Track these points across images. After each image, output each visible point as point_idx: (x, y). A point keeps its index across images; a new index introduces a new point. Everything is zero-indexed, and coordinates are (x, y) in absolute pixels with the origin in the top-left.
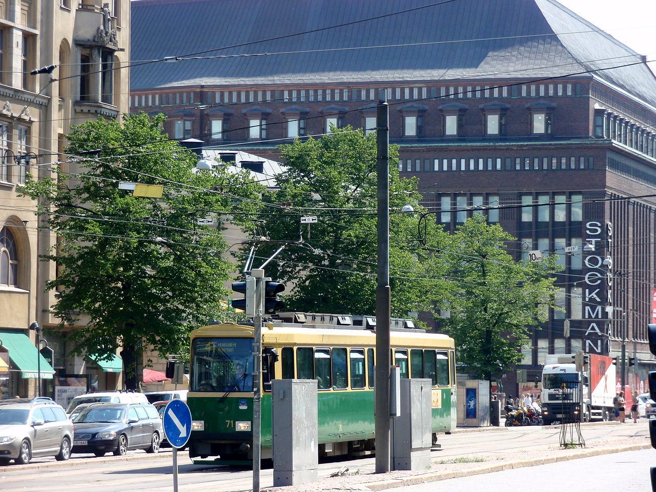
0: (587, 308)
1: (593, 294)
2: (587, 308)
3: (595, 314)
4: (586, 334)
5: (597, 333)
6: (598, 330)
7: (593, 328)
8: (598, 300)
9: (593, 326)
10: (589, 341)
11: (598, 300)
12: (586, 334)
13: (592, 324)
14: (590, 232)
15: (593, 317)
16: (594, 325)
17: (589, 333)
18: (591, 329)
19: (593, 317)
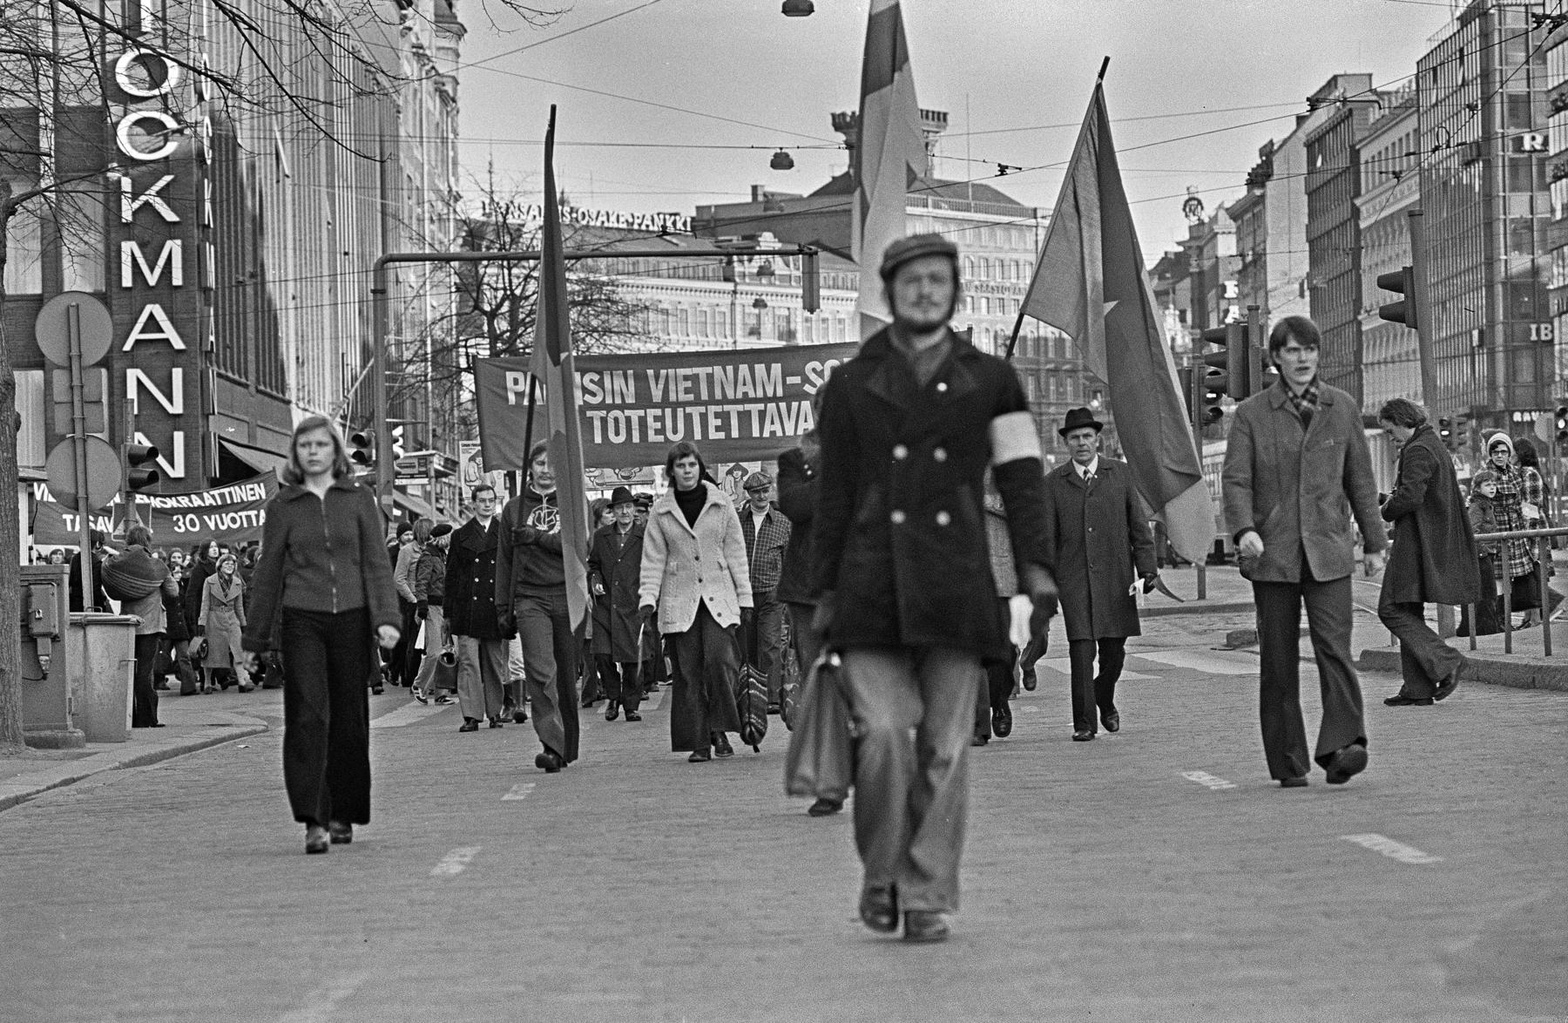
0: (129, 247)
1: (151, 196)
2: (129, 247)
3: (158, 271)
4: (127, 347)
5: (167, 341)
6: (170, 333)
8: (170, 216)
9: (151, 316)
10: (139, 373)
11: (170, 216)
12: (127, 347)
13: (149, 308)
15: (152, 279)
17: (138, 342)
18: (142, 331)
19: (152, 279)
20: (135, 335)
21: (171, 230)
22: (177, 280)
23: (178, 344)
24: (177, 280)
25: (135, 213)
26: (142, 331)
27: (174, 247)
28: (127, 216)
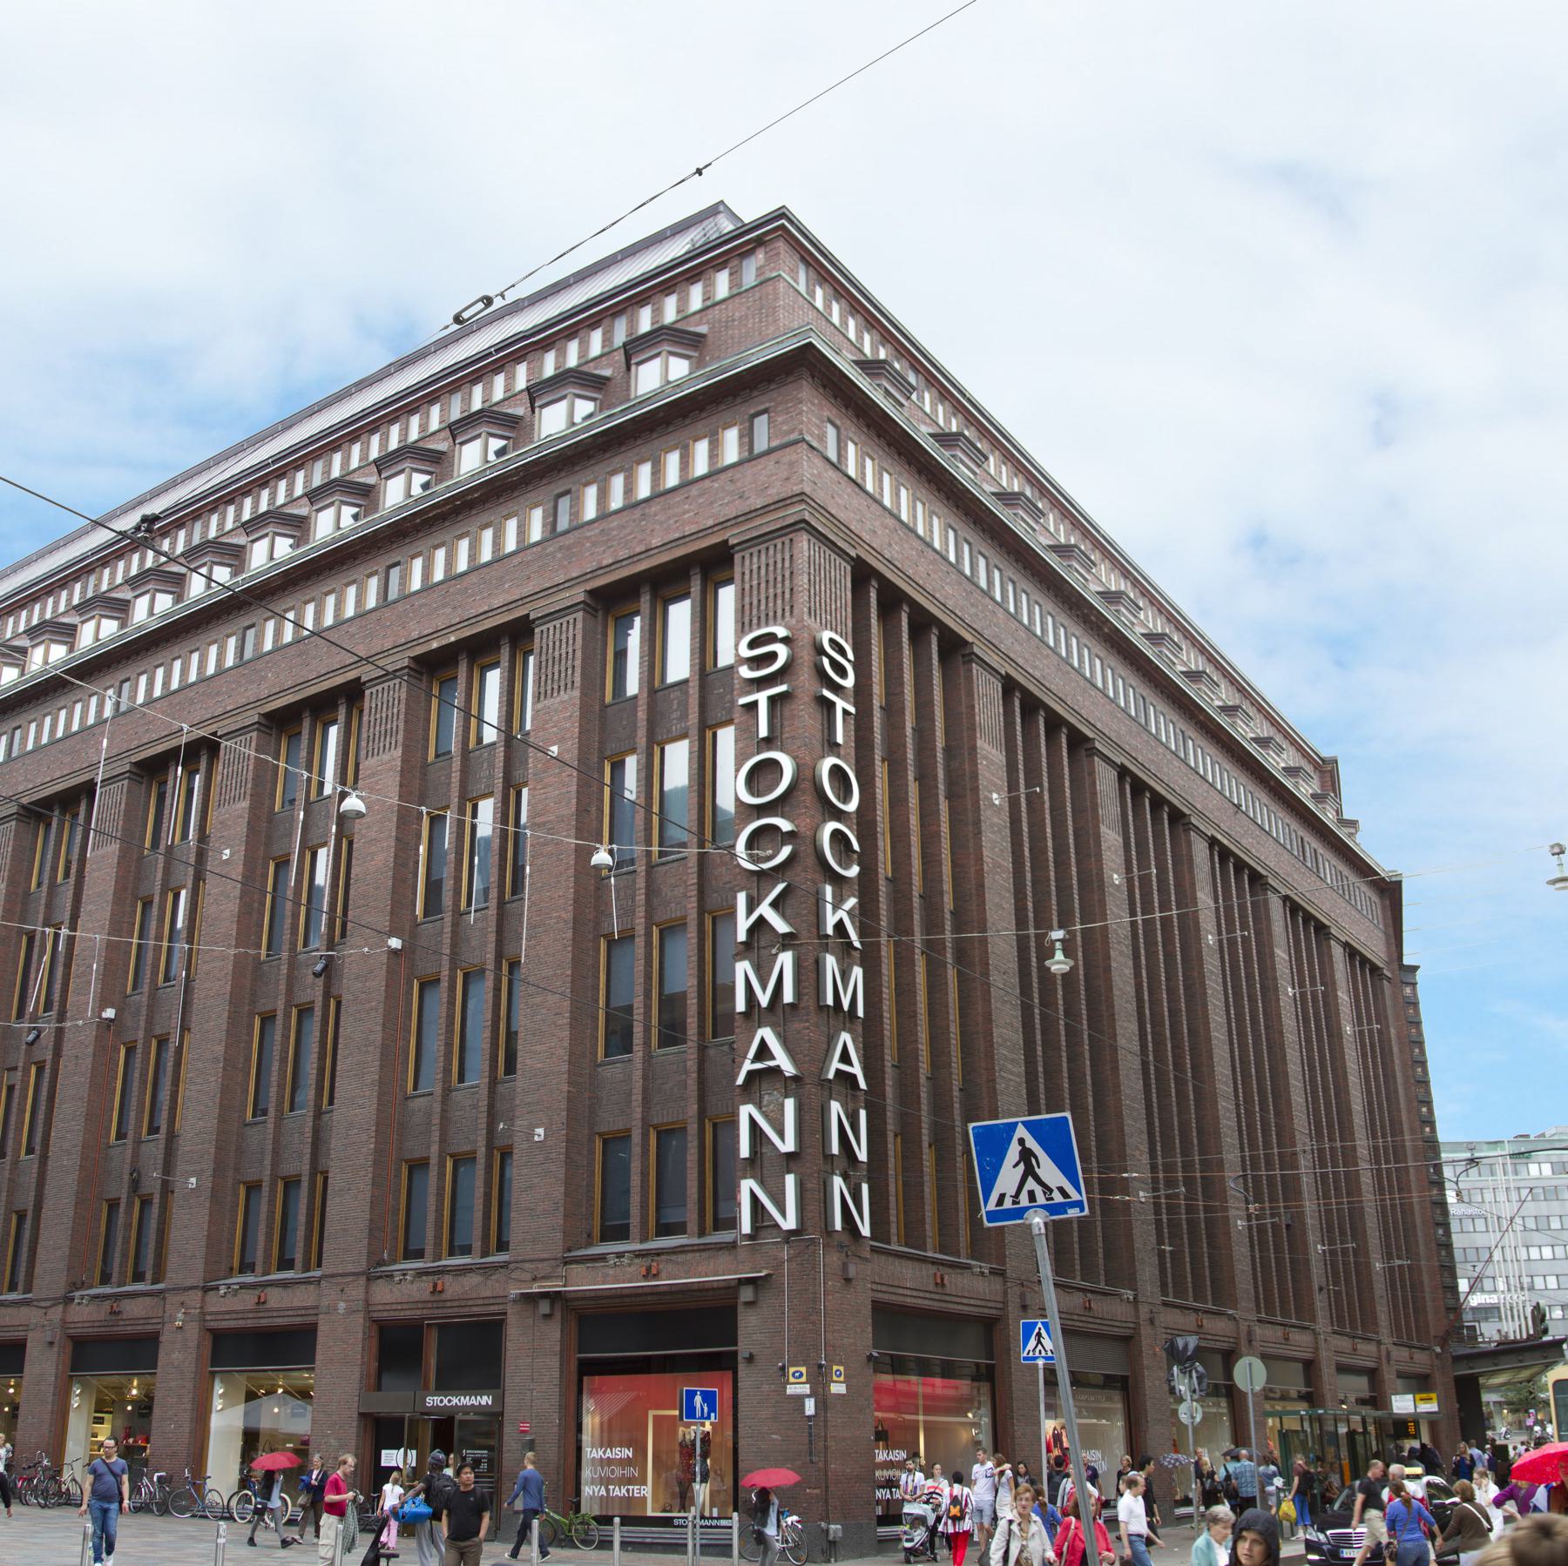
1: (765, 910)
5: (777, 1071)
7: (764, 1052)
8: (781, 926)
9: (763, 1043)
11: (781, 926)
12: (740, 1081)
14: (751, 669)
15: (764, 999)
16: (766, 1033)
17: (750, 1074)
19: (764, 999)
20: (748, 1066)
21: (787, 941)
22: (788, 996)
23: (788, 1068)
24: (788, 996)
25: (751, 931)
26: (753, 1062)
27: (786, 960)
28: (742, 936)
